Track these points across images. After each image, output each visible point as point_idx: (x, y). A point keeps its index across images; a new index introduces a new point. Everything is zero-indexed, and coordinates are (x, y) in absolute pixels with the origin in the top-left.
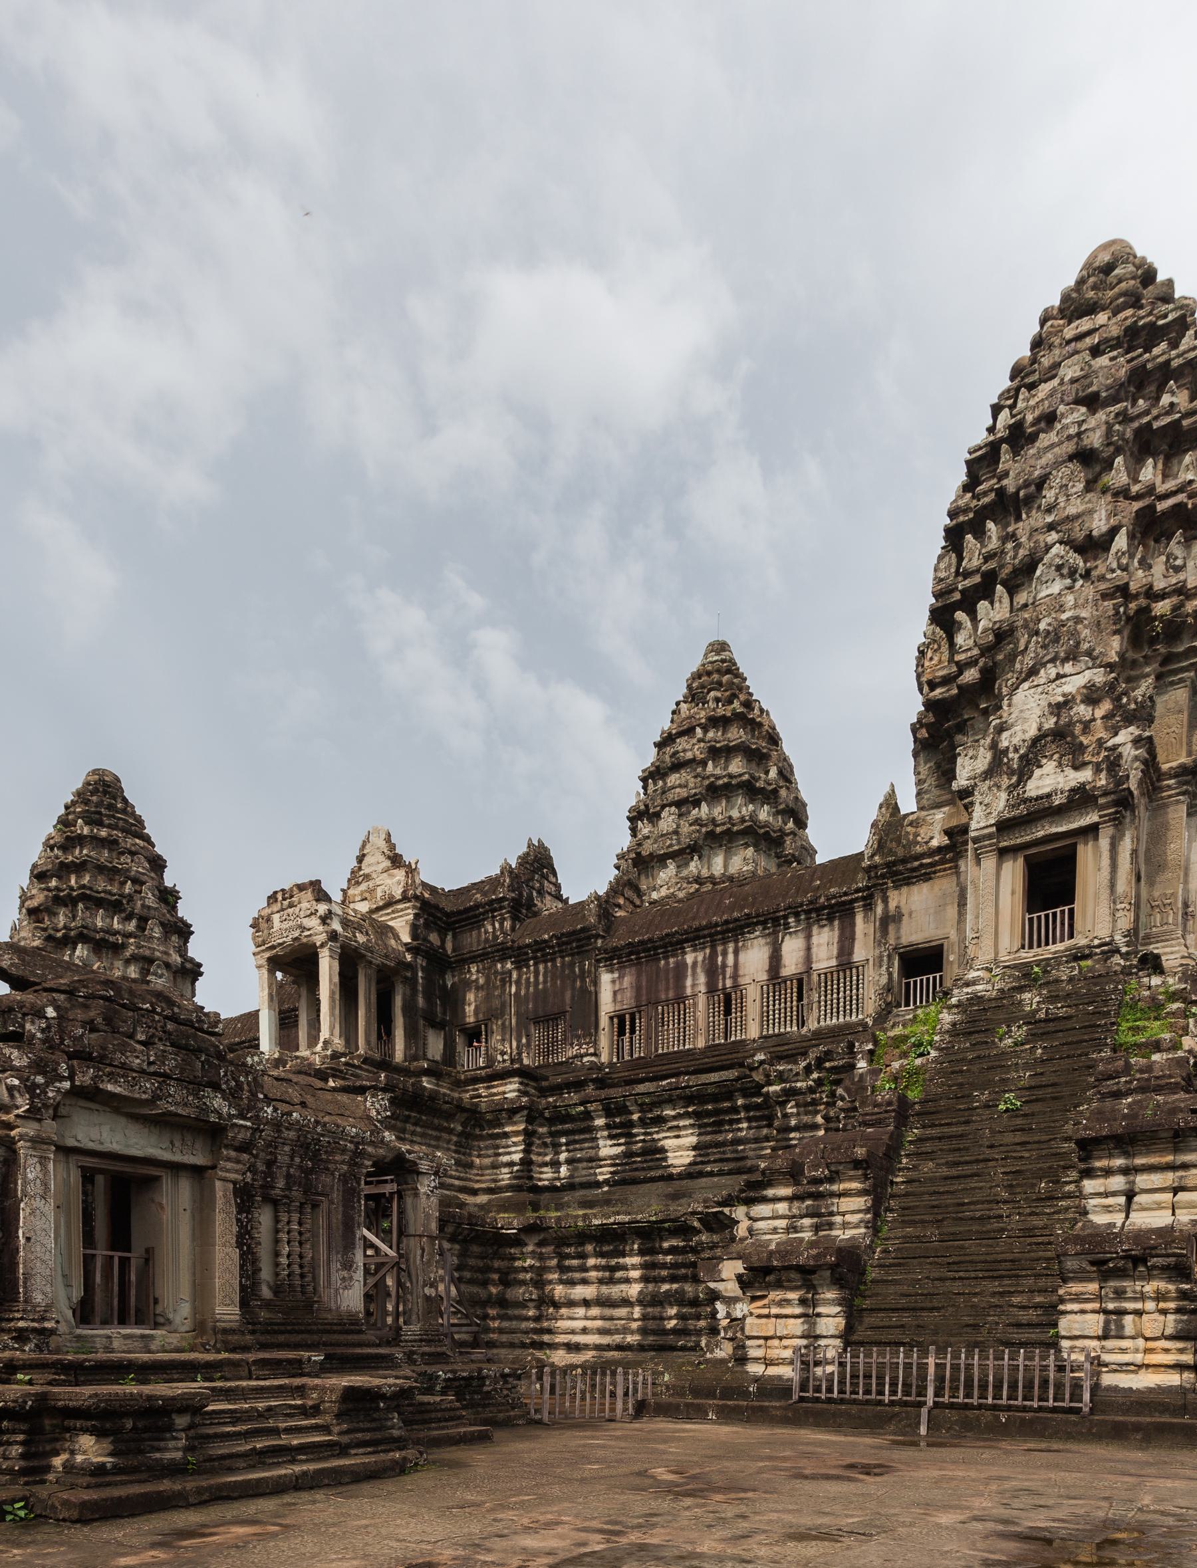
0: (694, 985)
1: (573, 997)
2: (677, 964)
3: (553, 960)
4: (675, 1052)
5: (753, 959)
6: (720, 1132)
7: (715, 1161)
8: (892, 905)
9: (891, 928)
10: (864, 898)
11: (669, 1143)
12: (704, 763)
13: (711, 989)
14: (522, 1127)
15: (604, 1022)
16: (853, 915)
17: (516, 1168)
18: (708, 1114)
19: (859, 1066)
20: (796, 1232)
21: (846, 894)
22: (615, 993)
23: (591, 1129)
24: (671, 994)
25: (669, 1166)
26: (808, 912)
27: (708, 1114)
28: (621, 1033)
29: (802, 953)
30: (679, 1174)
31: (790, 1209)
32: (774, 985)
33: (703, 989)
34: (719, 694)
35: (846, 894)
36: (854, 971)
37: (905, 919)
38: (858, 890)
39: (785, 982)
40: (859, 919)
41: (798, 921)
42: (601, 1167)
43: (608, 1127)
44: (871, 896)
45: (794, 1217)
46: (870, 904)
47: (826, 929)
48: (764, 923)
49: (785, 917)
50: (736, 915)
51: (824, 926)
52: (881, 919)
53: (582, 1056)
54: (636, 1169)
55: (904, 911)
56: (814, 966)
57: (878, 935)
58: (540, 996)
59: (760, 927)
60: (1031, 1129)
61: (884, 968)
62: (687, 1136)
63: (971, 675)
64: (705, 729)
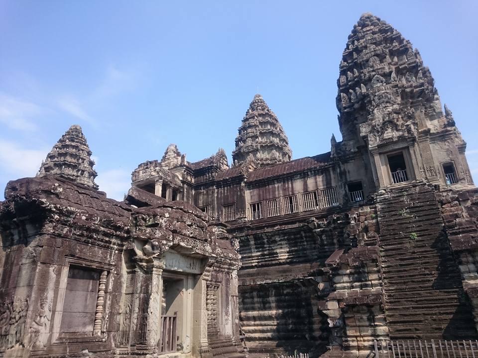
0: (279, 194)
1: (237, 198)
2: (272, 187)
3: (230, 186)
4: (274, 217)
5: (298, 185)
8: (342, 169)
9: (343, 176)
10: (332, 167)
13: (285, 196)
16: (330, 172)
19: (352, 222)
22: (251, 196)
24: (271, 197)
28: (254, 210)
29: (314, 184)
31: (350, 279)
32: (306, 194)
33: (282, 195)
35: (326, 165)
37: (347, 173)
38: (330, 164)
39: (310, 193)
41: (312, 174)
48: (300, 174)
49: (307, 172)
52: (339, 173)
55: (347, 171)
57: (339, 178)
58: (226, 198)
60: (426, 246)
61: (343, 189)
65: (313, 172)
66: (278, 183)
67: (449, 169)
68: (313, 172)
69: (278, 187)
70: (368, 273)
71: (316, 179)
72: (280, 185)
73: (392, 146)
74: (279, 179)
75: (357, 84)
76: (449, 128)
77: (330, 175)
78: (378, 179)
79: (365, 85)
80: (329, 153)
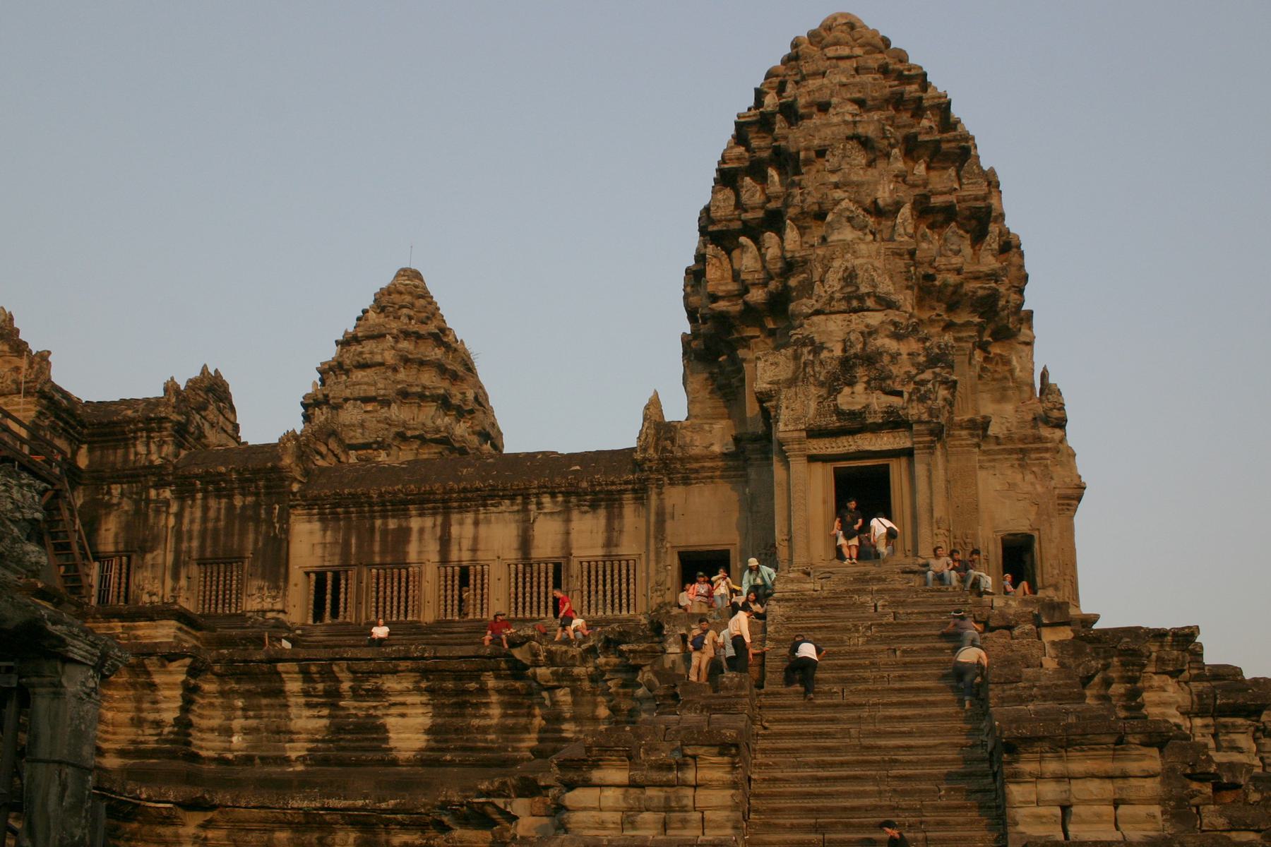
6: (463, 716)
7: (456, 749)
11: (391, 722)
12: (395, 370)
14: (183, 677)
15: (296, 574)
16: (621, 507)
17: (166, 730)
18: (446, 693)
19: (670, 650)
20: (634, 828)
21: (613, 483)
23: (280, 693)
25: (391, 749)
26: (567, 494)
27: (446, 693)
29: (559, 537)
30: (408, 760)
34: (412, 313)
36: (624, 564)
40: (629, 511)
42: (292, 741)
43: (306, 693)
44: (644, 490)
45: (631, 809)
46: (642, 498)
47: (589, 516)
48: (512, 498)
50: (478, 484)
51: (586, 512)
53: (264, 612)
54: (344, 749)
56: (575, 552)
59: (507, 502)
62: (417, 715)
63: (757, 295)
64: (396, 339)
65: (560, 499)
66: (421, 515)
67: (1018, 557)
68: (560, 499)
69: (421, 531)
70: (696, 787)
71: (568, 521)
72: (429, 522)
73: (860, 442)
74: (429, 501)
75: (774, 221)
76: (1045, 432)
77: (621, 516)
78: (790, 540)
79: (802, 230)
80: (632, 450)
